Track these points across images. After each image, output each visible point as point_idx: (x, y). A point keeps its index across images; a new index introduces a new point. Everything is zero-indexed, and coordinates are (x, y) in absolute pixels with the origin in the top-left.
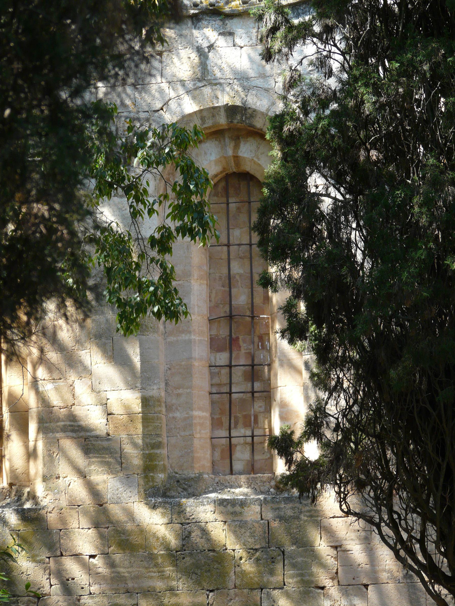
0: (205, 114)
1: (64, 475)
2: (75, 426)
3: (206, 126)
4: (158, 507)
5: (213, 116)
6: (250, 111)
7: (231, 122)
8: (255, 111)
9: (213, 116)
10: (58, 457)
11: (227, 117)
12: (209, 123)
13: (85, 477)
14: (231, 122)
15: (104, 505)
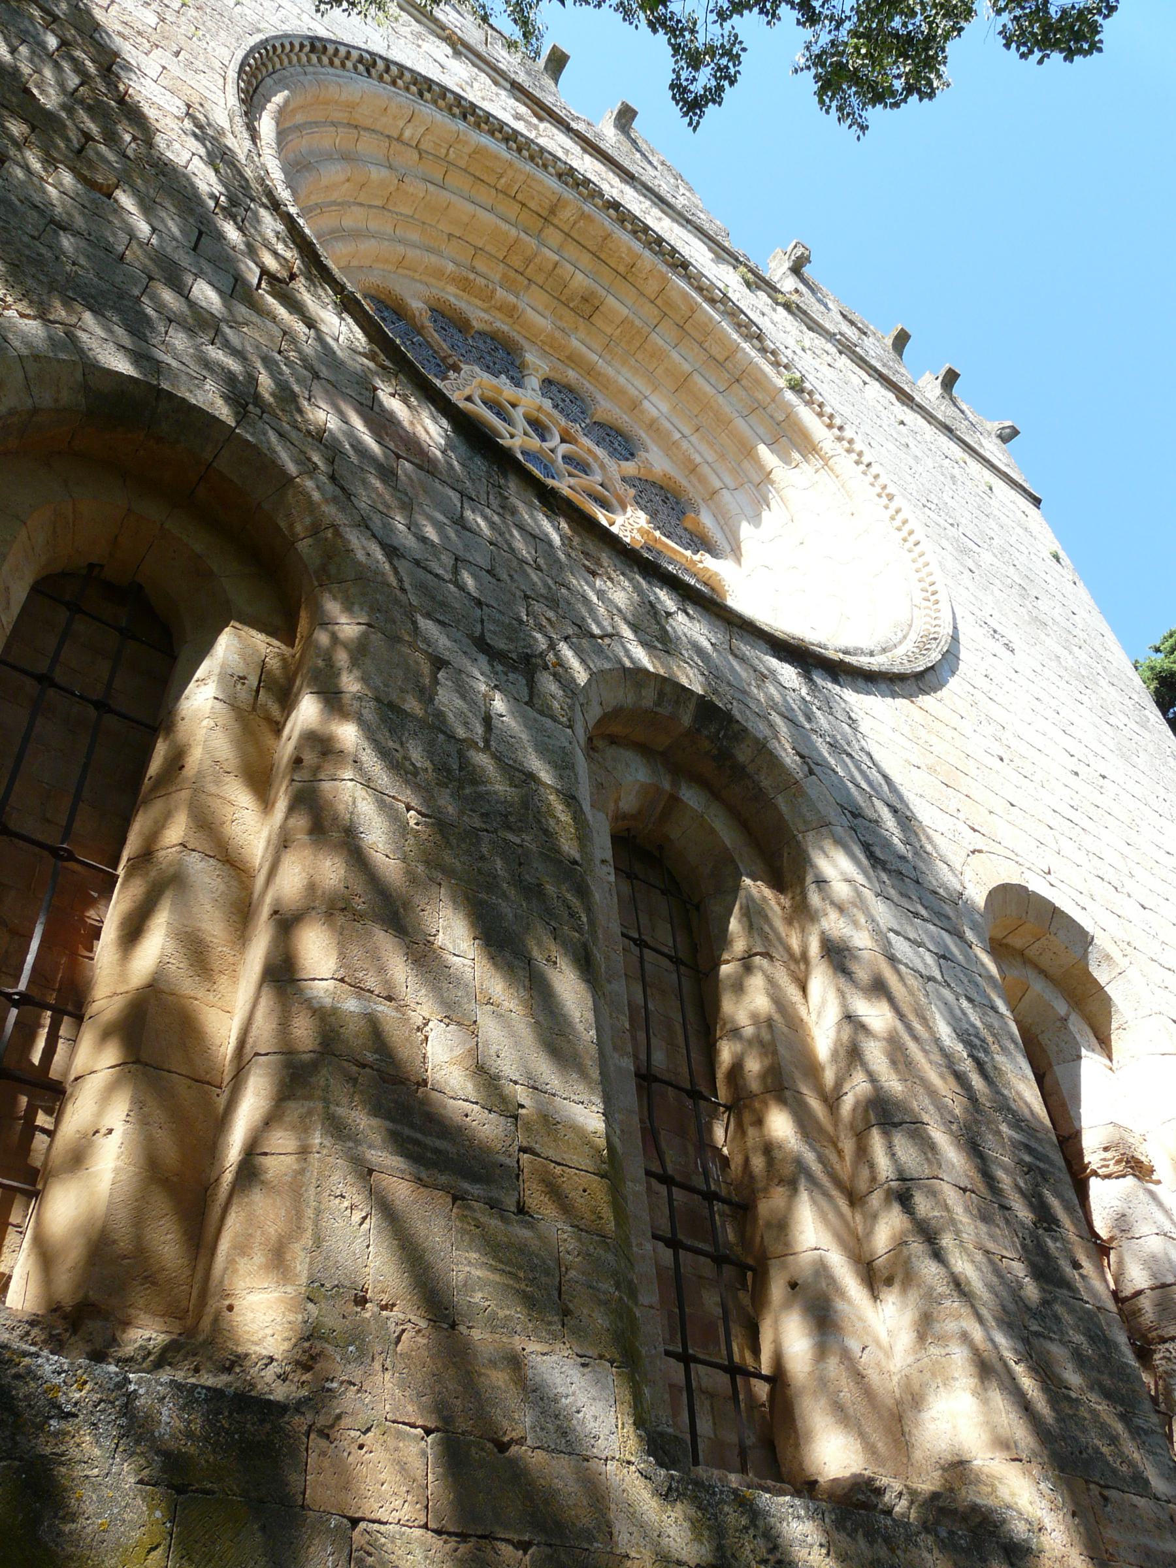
0: (668, 689)
1: (385, 1299)
2: (425, 1147)
3: (658, 709)
4: (681, 1496)
5: (677, 702)
6: (736, 727)
7: (698, 730)
8: (745, 730)
9: (677, 702)
10: (366, 1226)
11: (696, 718)
12: (665, 710)
13: (453, 1326)
14: (698, 730)
15: (514, 1449)
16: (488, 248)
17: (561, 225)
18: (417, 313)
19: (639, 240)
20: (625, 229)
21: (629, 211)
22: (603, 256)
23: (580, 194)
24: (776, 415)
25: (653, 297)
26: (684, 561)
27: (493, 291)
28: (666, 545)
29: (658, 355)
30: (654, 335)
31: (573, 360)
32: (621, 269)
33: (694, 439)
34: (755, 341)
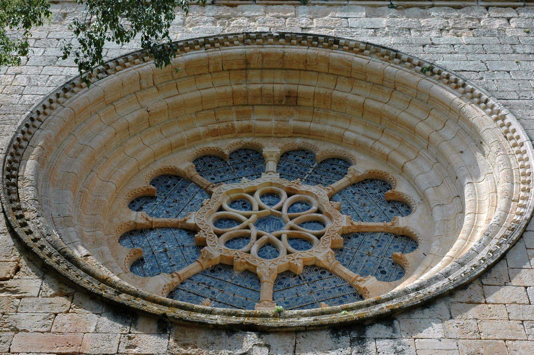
16: (221, 104)
17: (256, 66)
18: (186, 172)
19: (304, 45)
20: (293, 45)
21: (291, 33)
22: (288, 66)
23: (258, 44)
24: (423, 98)
25: (327, 71)
26: (382, 229)
27: (233, 126)
28: (367, 227)
29: (342, 102)
30: (335, 92)
31: (297, 133)
32: (302, 67)
33: (384, 139)
34: (396, 60)
